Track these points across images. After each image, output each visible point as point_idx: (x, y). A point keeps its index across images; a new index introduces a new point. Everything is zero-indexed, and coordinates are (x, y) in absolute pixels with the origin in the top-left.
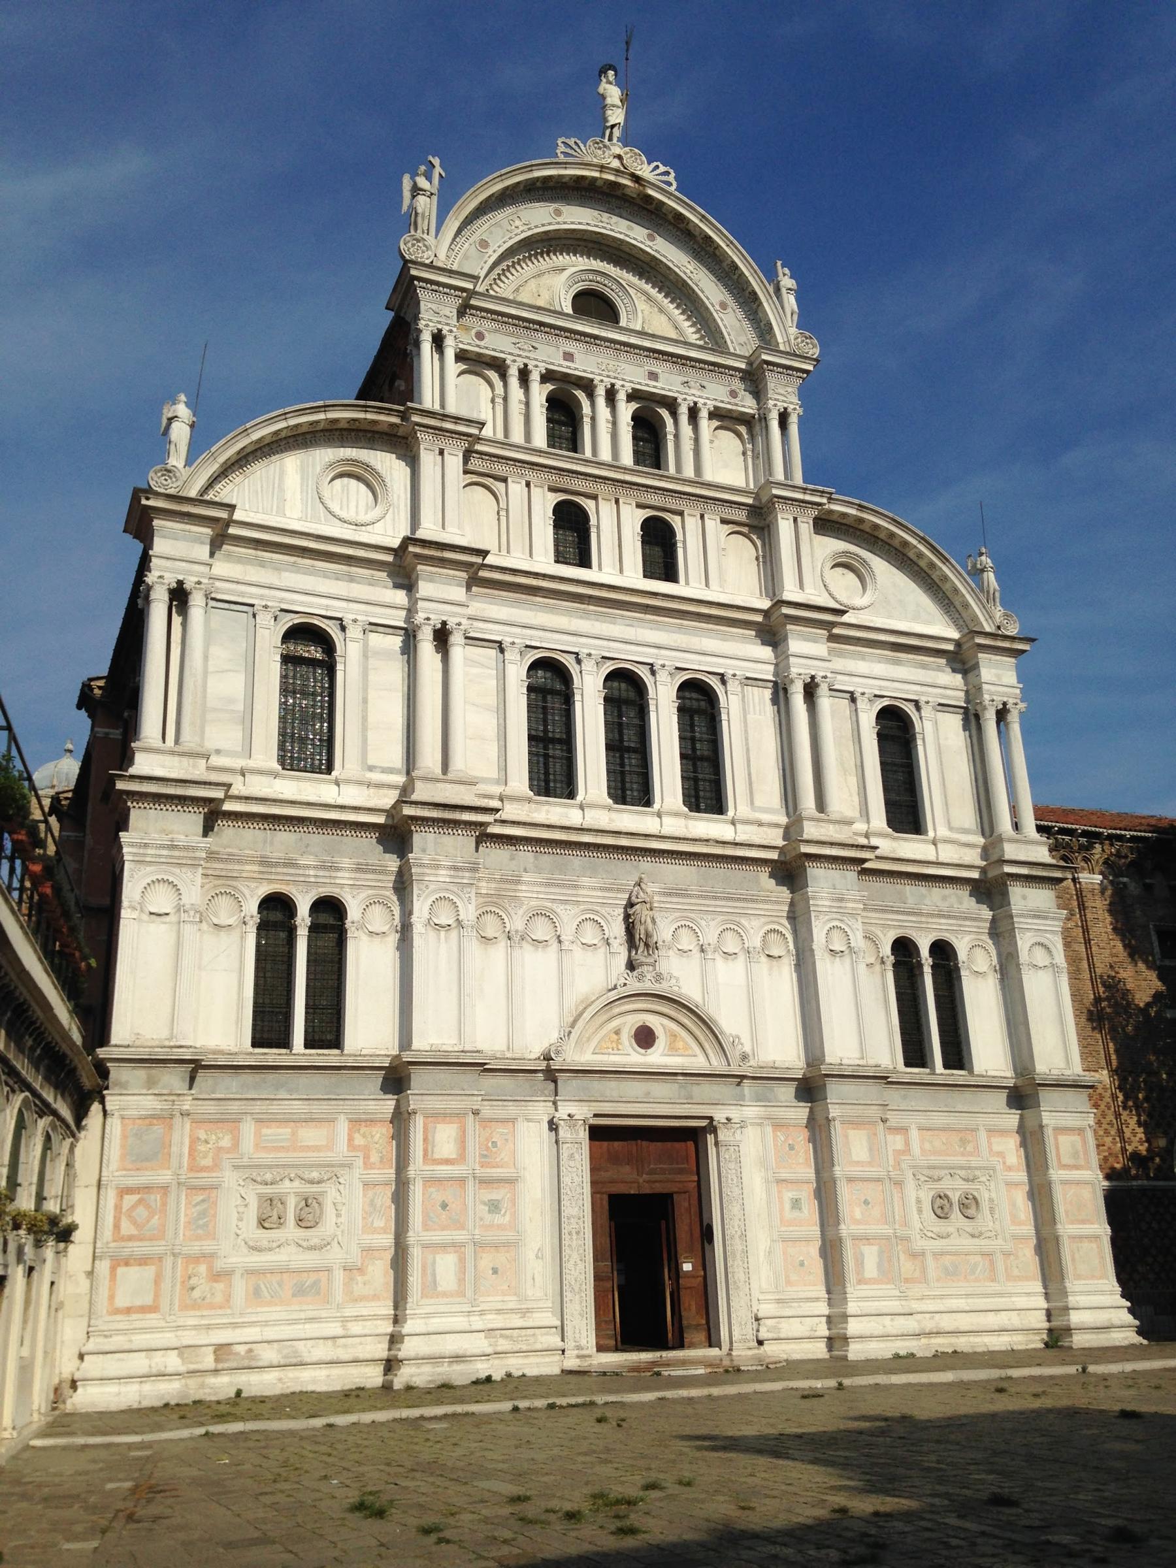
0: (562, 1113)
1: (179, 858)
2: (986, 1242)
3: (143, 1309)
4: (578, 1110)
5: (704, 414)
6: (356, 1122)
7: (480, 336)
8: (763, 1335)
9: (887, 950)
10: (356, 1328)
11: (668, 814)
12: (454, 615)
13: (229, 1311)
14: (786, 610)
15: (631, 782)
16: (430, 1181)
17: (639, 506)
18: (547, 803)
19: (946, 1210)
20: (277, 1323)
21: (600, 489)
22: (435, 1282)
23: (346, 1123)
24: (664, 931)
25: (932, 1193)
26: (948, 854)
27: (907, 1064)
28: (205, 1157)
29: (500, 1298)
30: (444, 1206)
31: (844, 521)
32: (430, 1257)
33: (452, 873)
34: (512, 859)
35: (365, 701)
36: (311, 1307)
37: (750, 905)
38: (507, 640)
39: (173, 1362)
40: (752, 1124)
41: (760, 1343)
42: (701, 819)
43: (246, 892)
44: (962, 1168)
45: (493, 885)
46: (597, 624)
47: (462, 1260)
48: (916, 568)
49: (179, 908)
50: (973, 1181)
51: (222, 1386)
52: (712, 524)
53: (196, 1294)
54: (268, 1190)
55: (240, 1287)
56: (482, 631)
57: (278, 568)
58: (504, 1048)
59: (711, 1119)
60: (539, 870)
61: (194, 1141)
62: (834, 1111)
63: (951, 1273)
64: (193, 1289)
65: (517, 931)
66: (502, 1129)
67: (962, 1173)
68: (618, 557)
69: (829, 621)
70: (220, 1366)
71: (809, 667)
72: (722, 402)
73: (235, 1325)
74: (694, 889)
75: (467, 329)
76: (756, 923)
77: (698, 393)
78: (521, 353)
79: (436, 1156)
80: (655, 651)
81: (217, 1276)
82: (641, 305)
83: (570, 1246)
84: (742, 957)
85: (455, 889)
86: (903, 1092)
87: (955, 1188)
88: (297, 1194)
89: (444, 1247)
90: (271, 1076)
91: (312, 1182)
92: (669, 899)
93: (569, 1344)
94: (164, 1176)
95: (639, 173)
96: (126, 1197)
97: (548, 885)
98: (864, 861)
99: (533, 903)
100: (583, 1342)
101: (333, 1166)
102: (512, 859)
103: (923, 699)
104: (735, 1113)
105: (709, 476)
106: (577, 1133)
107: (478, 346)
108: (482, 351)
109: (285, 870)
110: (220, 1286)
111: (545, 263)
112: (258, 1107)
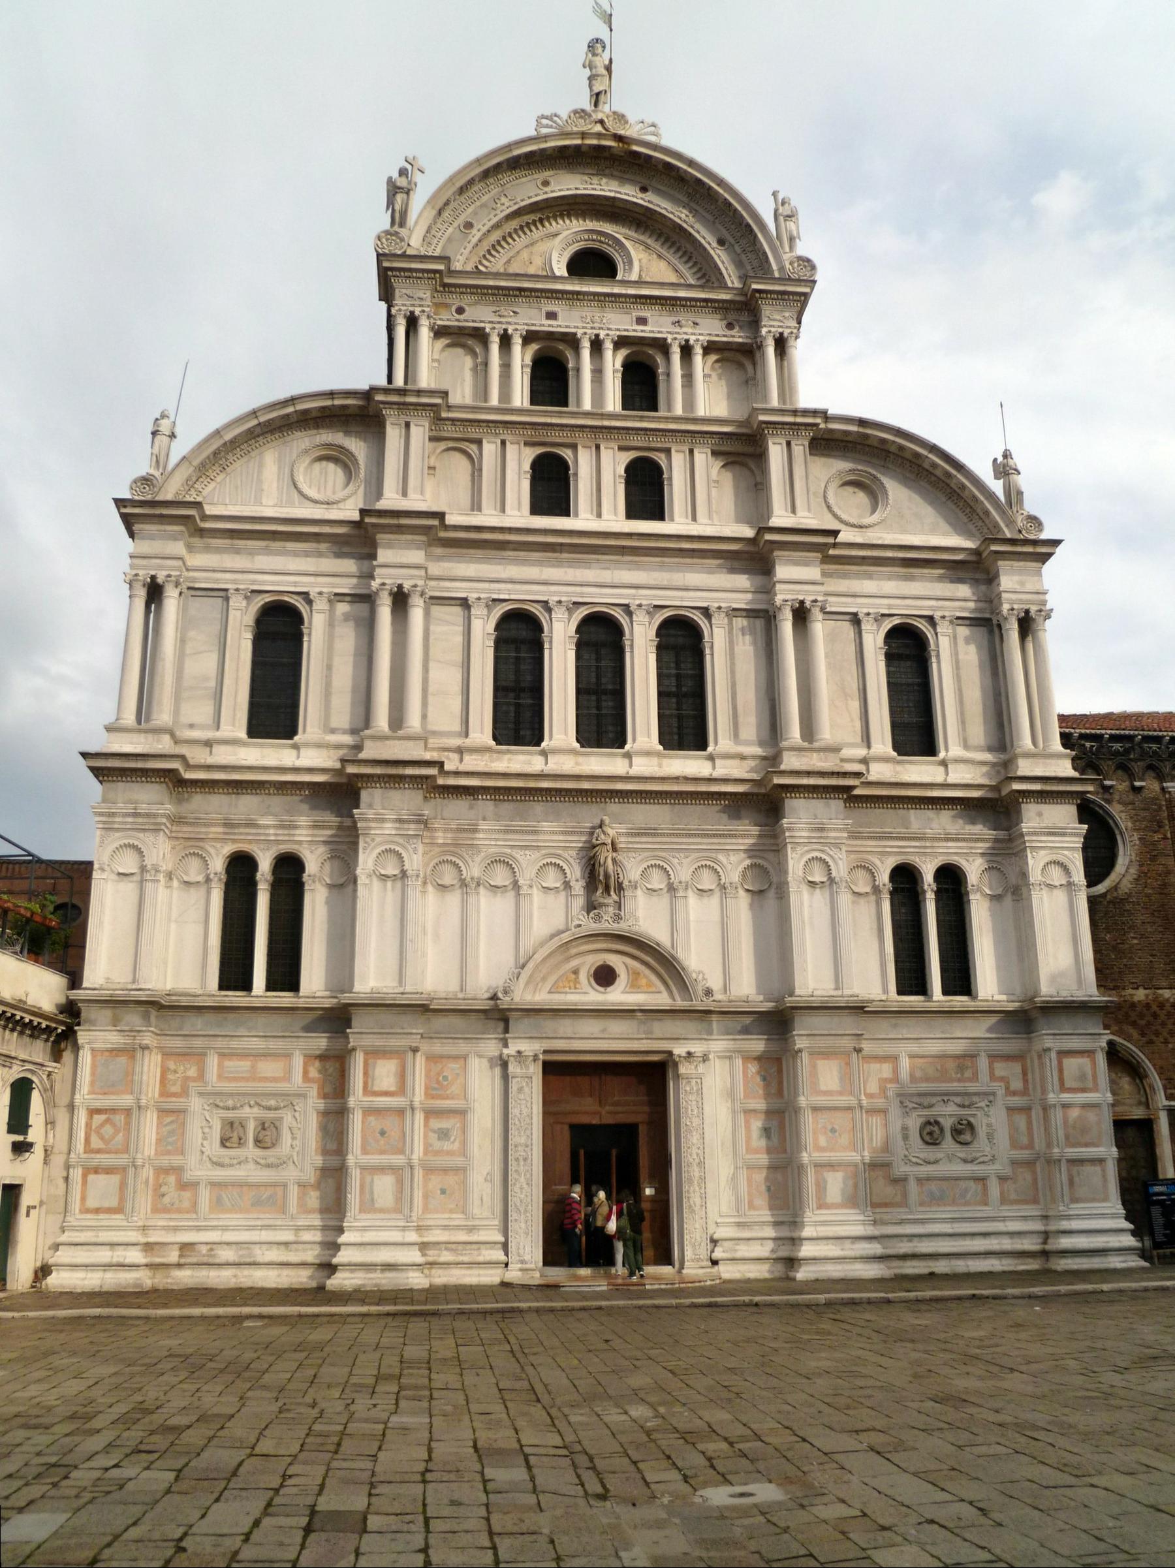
0: (511, 1050)
1: (142, 824)
2: (982, 1167)
3: (110, 1211)
4: (526, 1046)
5: (698, 351)
6: (309, 1058)
7: (460, 311)
8: (718, 1254)
9: (884, 878)
10: (307, 1236)
11: (644, 754)
12: (412, 577)
13: (194, 1216)
14: (768, 537)
15: (603, 723)
16: (369, 1111)
17: (621, 449)
18: (509, 752)
19: (936, 1136)
20: (236, 1228)
21: (580, 439)
22: (372, 1200)
23: (302, 1058)
24: (632, 869)
25: (922, 1120)
26: (958, 775)
27: (900, 993)
28: (174, 1084)
29: (447, 1216)
30: (383, 1133)
31: (850, 438)
32: (368, 1179)
33: (397, 825)
34: (471, 808)
35: (329, 667)
36: (268, 1216)
37: (728, 841)
38: (472, 596)
39: (135, 1256)
40: (719, 1057)
41: (715, 1263)
42: (677, 757)
43: (212, 851)
44: (957, 1094)
45: (449, 835)
46: (570, 571)
47: (400, 1182)
48: (933, 478)
49: (143, 869)
50: (969, 1106)
51: (185, 1277)
52: (702, 457)
53: (166, 1200)
54: (230, 1114)
55: (205, 1196)
56: (448, 589)
57: (252, 553)
58: (458, 989)
59: (670, 1053)
60: (498, 818)
61: (164, 1071)
62: (800, 1043)
63: (937, 1200)
64: (163, 1195)
65: (472, 878)
66: (454, 1066)
67: (958, 1100)
68: (598, 502)
69: (821, 545)
70: (183, 1261)
71: (798, 592)
72: (717, 335)
73: (198, 1229)
74: (665, 827)
75: (447, 306)
76: (734, 858)
77: (690, 330)
78: (502, 320)
79: (376, 1089)
80: (633, 591)
81: (183, 1186)
82: (638, 254)
83: (516, 1171)
84: (717, 894)
85: (401, 841)
86: (893, 1021)
87: (947, 1114)
88: (256, 1119)
89: (381, 1169)
90: (231, 1016)
91: (269, 1108)
92: (637, 839)
93: (513, 1257)
94: (127, 1100)
95: (622, 132)
96: (96, 1117)
97: (507, 832)
98: (854, 787)
99: (492, 850)
100: (527, 1258)
101: (288, 1095)
102: (471, 808)
103: (937, 615)
104: (697, 1048)
105: (701, 411)
106: (527, 1068)
107: (458, 320)
108: (461, 324)
109: (247, 830)
110: (187, 1195)
111: (536, 234)
112: (219, 1043)
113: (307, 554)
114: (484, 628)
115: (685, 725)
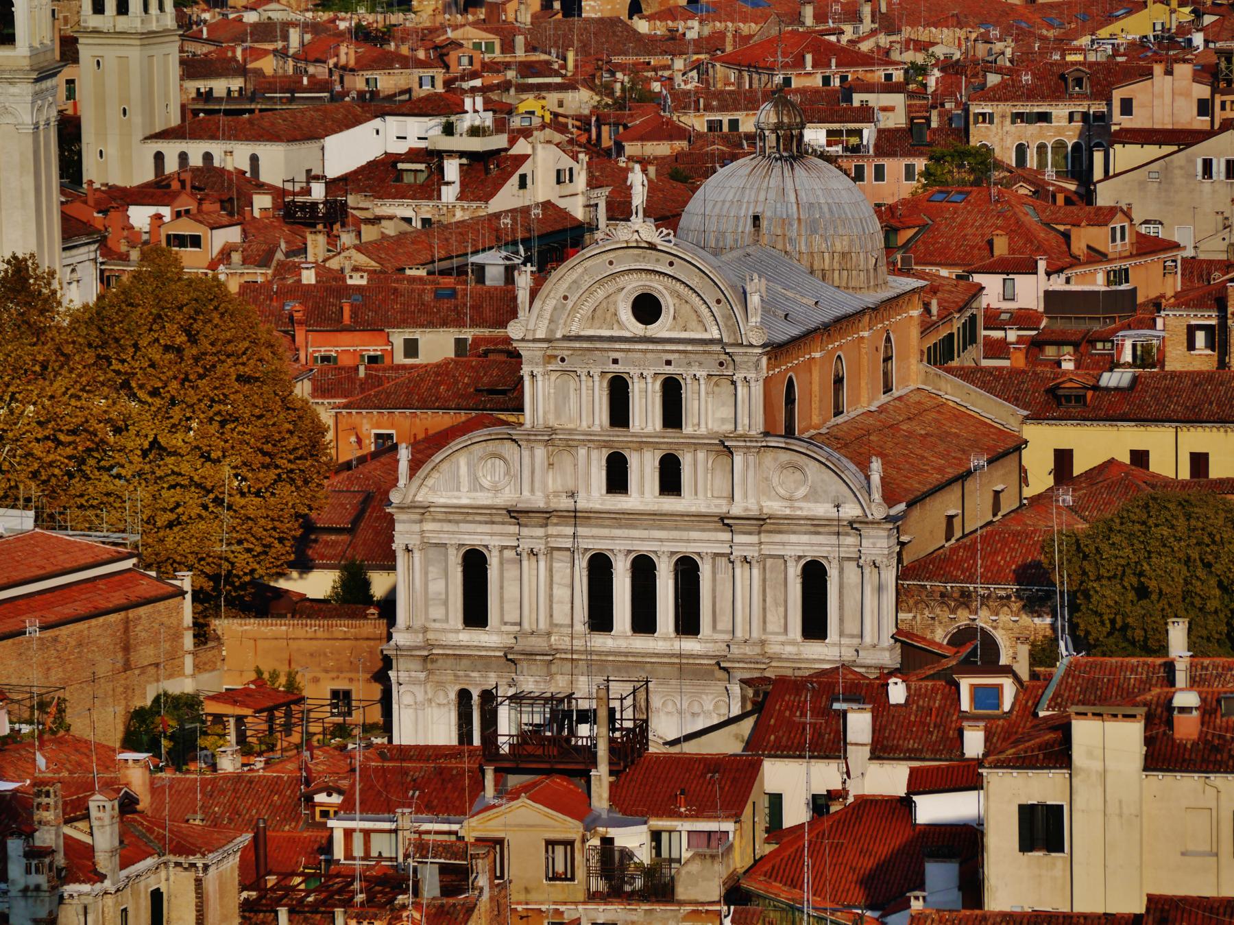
15: (644, 622)
35: (502, 588)
52: (701, 455)
57: (457, 522)
76: (710, 697)
113: (486, 523)
114: (582, 563)
115: (688, 623)
